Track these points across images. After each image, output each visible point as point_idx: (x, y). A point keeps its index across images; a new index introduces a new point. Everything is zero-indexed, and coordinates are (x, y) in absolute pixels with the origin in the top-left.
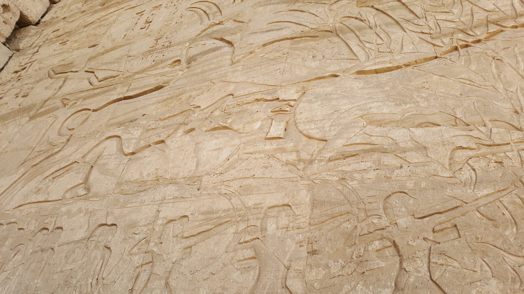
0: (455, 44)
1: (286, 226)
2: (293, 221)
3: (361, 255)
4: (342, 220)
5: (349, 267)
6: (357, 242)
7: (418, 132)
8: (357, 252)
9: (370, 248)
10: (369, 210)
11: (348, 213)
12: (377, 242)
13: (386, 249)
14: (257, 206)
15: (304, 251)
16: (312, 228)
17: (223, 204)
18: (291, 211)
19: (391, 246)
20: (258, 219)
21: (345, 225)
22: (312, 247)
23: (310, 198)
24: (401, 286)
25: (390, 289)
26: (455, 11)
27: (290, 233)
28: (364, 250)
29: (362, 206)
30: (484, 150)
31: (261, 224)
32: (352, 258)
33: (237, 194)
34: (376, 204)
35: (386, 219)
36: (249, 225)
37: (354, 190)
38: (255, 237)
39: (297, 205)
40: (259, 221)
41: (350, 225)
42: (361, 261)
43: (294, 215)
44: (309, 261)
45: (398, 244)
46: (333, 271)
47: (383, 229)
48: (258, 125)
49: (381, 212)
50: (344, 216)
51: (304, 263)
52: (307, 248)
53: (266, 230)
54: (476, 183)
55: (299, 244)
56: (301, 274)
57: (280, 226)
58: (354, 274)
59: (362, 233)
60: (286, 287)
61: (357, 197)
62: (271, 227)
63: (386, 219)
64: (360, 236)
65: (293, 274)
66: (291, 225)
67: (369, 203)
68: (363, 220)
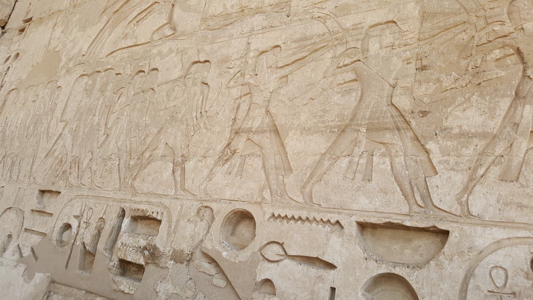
1: (391, 45)
2: (399, 38)
3: (478, 66)
4: (457, 31)
5: (463, 79)
6: (474, 53)
8: (473, 63)
9: (488, 58)
10: (490, 17)
11: (464, 22)
12: (497, 51)
13: (507, 58)
14: (356, 27)
15: (412, 68)
16: (421, 43)
17: (318, 28)
18: (397, 28)
19: (513, 54)
20: (358, 40)
21: (460, 36)
22: (422, 62)
23: (419, 11)
24: (522, 94)
25: (510, 98)
27: (395, 51)
28: (482, 61)
29: (481, 13)
31: (362, 45)
32: (467, 70)
33: (332, 15)
34: (500, 8)
35: (510, 25)
36: (348, 48)
38: (355, 59)
39: (403, 20)
40: (360, 43)
41: (466, 36)
42: (477, 72)
43: (401, 31)
44: (418, 77)
45: (522, 51)
46: (444, 84)
47: (506, 36)
49: (505, 17)
50: (458, 27)
51: (413, 80)
52: (416, 65)
53: (368, 50)
55: (406, 62)
56: (409, 91)
57: (385, 44)
58: (468, 86)
59: (480, 43)
60: (393, 104)
61: (476, 4)
62: (374, 46)
63: (510, 25)
64: (477, 46)
65: (399, 91)
66: (397, 42)
67: (491, 9)
68: (482, 29)
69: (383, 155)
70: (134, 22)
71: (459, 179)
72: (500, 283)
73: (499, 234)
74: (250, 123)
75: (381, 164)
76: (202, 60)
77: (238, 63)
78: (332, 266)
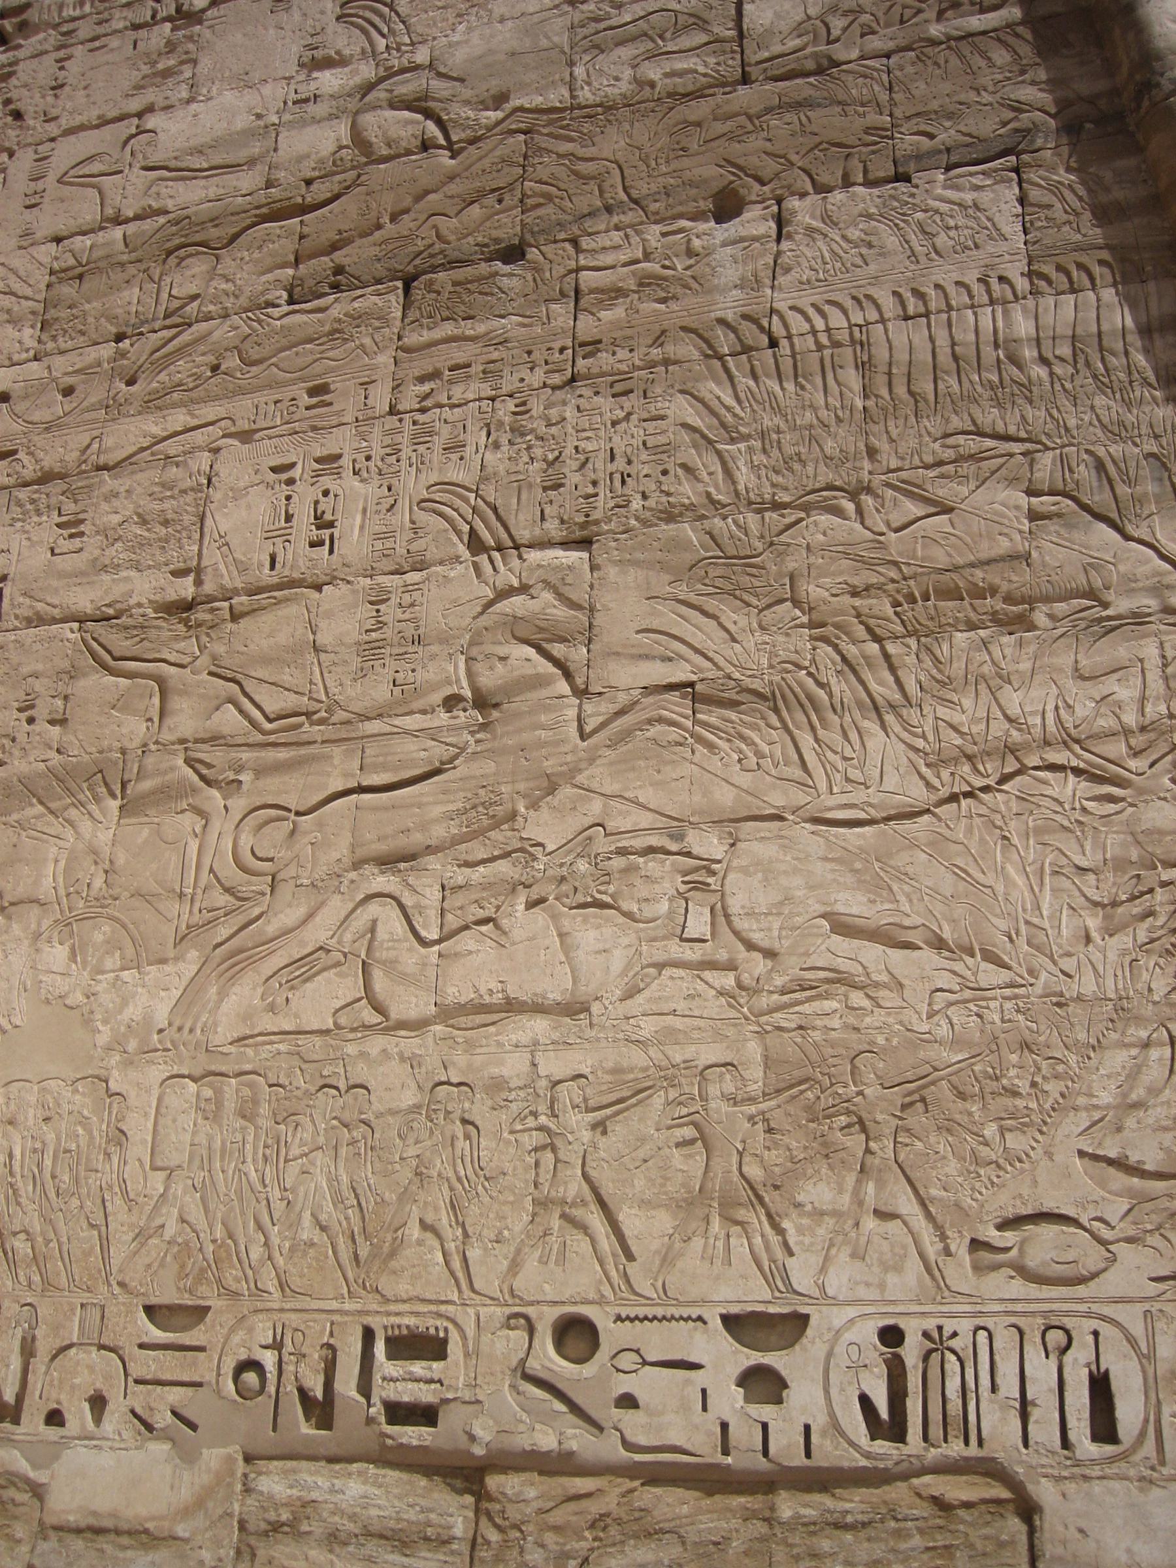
0: (956, 790)
7: (896, 955)
30: (968, 994)
37: (816, 1045)
48: (664, 907)
69: (740, 1236)
70: (284, 976)
71: (816, 1260)
72: (855, 1358)
73: (851, 1312)
74: (561, 1189)
75: (739, 1245)
76: (455, 1080)
77: (522, 1094)
78: (696, 1366)
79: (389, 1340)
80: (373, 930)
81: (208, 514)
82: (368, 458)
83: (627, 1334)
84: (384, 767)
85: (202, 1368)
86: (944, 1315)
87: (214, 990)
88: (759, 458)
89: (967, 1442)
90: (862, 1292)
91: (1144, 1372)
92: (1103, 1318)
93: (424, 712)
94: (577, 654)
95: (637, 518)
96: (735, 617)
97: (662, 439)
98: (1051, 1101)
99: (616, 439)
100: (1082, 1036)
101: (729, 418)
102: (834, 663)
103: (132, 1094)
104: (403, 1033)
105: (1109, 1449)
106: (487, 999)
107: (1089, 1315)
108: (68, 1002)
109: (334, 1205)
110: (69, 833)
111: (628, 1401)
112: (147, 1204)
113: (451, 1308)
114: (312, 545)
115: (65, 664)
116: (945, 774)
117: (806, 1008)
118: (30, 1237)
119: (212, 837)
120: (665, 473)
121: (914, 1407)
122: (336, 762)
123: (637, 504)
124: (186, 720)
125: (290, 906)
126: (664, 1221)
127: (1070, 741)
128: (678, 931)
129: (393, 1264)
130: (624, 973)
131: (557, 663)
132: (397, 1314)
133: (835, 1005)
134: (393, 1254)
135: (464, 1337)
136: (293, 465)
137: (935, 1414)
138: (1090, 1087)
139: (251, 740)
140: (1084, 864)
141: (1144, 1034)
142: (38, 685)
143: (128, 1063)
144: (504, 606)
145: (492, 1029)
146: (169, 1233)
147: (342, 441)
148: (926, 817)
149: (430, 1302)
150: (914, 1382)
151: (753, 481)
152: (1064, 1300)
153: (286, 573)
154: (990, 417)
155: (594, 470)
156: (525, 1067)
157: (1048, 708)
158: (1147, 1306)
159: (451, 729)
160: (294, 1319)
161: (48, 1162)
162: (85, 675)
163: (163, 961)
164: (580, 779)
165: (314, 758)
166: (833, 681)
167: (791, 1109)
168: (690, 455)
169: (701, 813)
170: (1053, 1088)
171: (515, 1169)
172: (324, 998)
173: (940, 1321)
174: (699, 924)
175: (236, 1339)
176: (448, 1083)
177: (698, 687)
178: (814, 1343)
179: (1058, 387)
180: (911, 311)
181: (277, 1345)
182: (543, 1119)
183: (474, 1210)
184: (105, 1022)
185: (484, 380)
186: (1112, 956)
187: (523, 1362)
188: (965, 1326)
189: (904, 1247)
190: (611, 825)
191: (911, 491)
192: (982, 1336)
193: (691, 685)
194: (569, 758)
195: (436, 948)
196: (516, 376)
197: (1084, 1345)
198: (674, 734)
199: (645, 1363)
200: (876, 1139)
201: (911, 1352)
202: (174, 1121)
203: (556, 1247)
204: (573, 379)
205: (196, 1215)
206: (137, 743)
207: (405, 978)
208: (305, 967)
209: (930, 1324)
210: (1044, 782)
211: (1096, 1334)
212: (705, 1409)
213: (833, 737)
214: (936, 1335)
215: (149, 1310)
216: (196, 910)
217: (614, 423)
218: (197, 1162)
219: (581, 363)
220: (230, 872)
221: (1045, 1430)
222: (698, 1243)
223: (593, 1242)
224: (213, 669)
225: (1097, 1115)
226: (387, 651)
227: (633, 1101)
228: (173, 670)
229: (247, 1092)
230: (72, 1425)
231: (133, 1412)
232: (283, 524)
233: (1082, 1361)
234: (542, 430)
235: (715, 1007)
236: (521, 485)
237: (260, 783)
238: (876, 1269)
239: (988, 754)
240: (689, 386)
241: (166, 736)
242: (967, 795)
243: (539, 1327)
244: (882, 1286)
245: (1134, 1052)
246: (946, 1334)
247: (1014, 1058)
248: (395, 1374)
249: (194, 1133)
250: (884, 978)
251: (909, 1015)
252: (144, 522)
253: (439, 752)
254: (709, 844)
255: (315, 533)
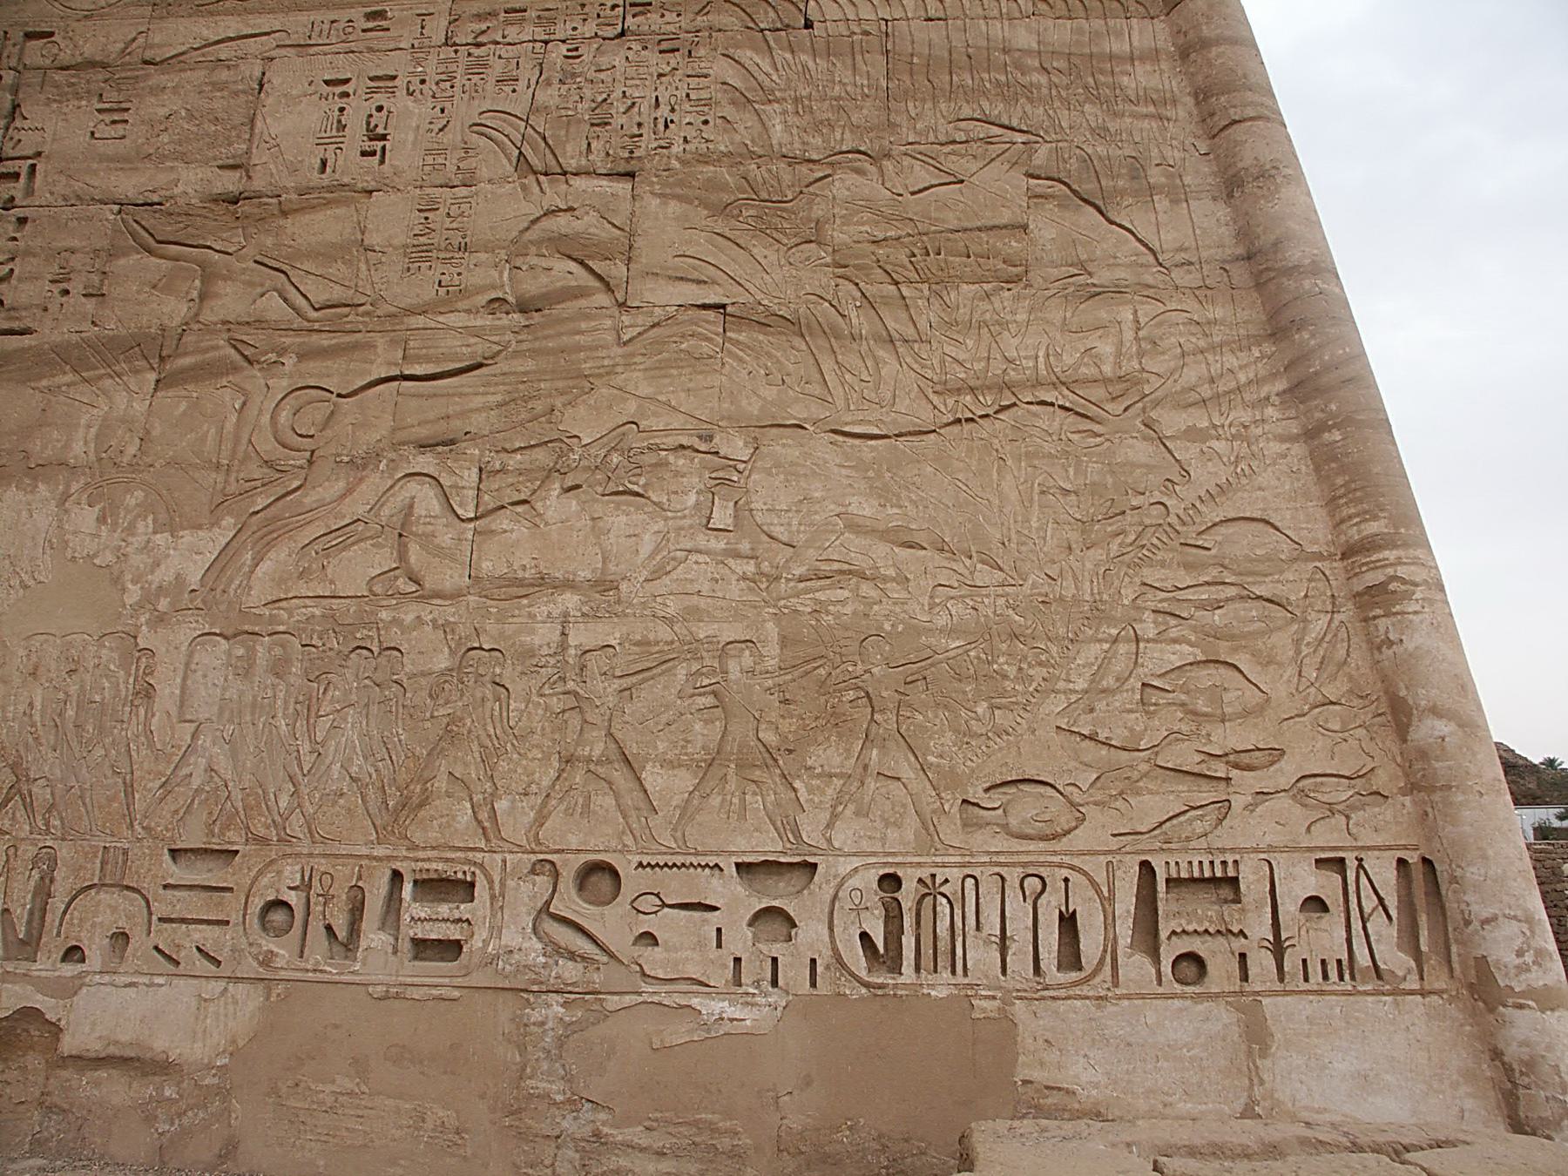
26: (970, 343)
30: (965, 591)
48: (692, 499)
54: (951, 632)
69: (755, 794)
73: (857, 862)
75: (755, 802)
77: (552, 661)
78: (716, 909)
79: (415, 882)
80: (411, 506)
81: (259, 117)
82: (423, 82)
83: (647, 879)
84: (428, 359)
85: (231, 907)
86: (936, 865)
87: (248, 557)
88: (792, 119)
89: (954, 972)
90: (865, 845)
91: (1104, 911)
92: (1072, 868)
93: (468, 311)
94: (617, 270)
95: (678, 158)
96: (766, 252)
97: (704, 94)
98: (1034, 685)
99: (661, 88)
100: (1062, 631)
101: (767, 82)
102: (854, 299)
103: (161, 650)
104: (439, 602)
105: (1074, 976)
106: (520, 574)
107: (1060, 866)
108: (97, 561)
109: (365, 758)
110: (102, 400)
111: (649, 938)
112: (174, 754)
113: (479, 855)
114: (364, 154)
115: (105, 243)
116: (950, 402)
117: (820, 596)
118: (50, 784)
119: (252, 411)
120: (706, 122)
121: (908, 942)
122: (379, 350)
123: (677, 149)
124: (230, 302)
125: (328, 480)
126: (685, 781)
127: (1059, 383)
128: (704, 521)
129: (422, 813)
130: (651, 556)
131: (599, 277)
132: (423, 860)
133: (846, 593)
134: (421, 805)
135: (491, 882)
136: (347, 81)
137: (927, 951)
138: (1068, 674)
139: (295, 326)
140: (1068, 487)
141: (1114, 632)
142: (76, 261)
143: (160, 620)
144: (548, 224)
145: (525, 601)
146: (196, 782)
147: (397, 64)
148: (932, 436)
149: (459, 849)
150: (908, 921)
151: (786, 138)
152: (1041, 853)
153: (337, 176)
154: (997, 109)
155: (639, 113)
156: (556, 637)
157: (1041, 354)
158: (1110, 858)
159: (494, 328)
160: (322, 865)
161: (71, 713)
162: (125, 255)
163: (200, 527)
164: (619, 380)
165: (356, 346)
166: (853, 314)
167: (804, 682)
168: (729, 111)
169: (729, 418)
170: (1038, 673)
171: (543, 729)
172: (360, 567)
173: (933, 871)
174: (722, 516)
175: (265, 881)
176: (481, 648)
177: (729, 309)
178: (822, 886)
179: (1054, 92)
180: (932, 13)
181: (306, 886)
182: (571, 685)
183: (503, 765)
184: (134, 582)
185: (537, 25)
186: (1089, 565)
187: (548, 903)
188: (955, 874)
189: (904, 806)
190: (643, 424)
191: (928, 159)
192: (970, 882)
193: (724, 306)
194: (606, 362)
195: (471, 525)
196: (569, 26)
197: (1056, 890)
198: (706, 348)
199: (664, 905)
200: (882, 711)
201: (907, 896)
202: (205, 676)
203: (581, 800)
204: (622, 34)
205: (224, 766)
206: (177, 321)
207: (440, 552)
208: (342, 536)
209: (925, 873)
210: (1035, 415)
211: (1066, 880)
212: (719, 946)
213: (852, 360)
214: (929, 882)
215: (174, 853)
216: (232, 479)
217: (660, 75)
218: (227, 715)
219: (630, 21)
220: (267, 446)
221: (1019, 961)
222: (716, 801)
223: (617, 797)
224: (258, 258)
225: (1073, 698)
226: (434, 254)
227: (659, 670)
228: (217, 256)
229: (278, 651)
230: (94, 959)
231: (156, 948)
232: (334, 133)
233: (1054, 903)
234: (591, 74)
235: (735, 590)
236: (570, 121)
237: (303, 366)
238: (879, 824)
239: (989, 388)
240: (731, 51)
241: (207, 316)
242: (968, 420)
243: (564, 873)
244: (883, 839)
245: (1106, 646)
246: (938, 882)
247: (1004, 646)
248: (423, 915)
249: (224, 689)
250: (891, 572)
251: (913, 607)
252: (191, 116)
253: (480, 348)
254: (736, 447)
255: (368, 145)
